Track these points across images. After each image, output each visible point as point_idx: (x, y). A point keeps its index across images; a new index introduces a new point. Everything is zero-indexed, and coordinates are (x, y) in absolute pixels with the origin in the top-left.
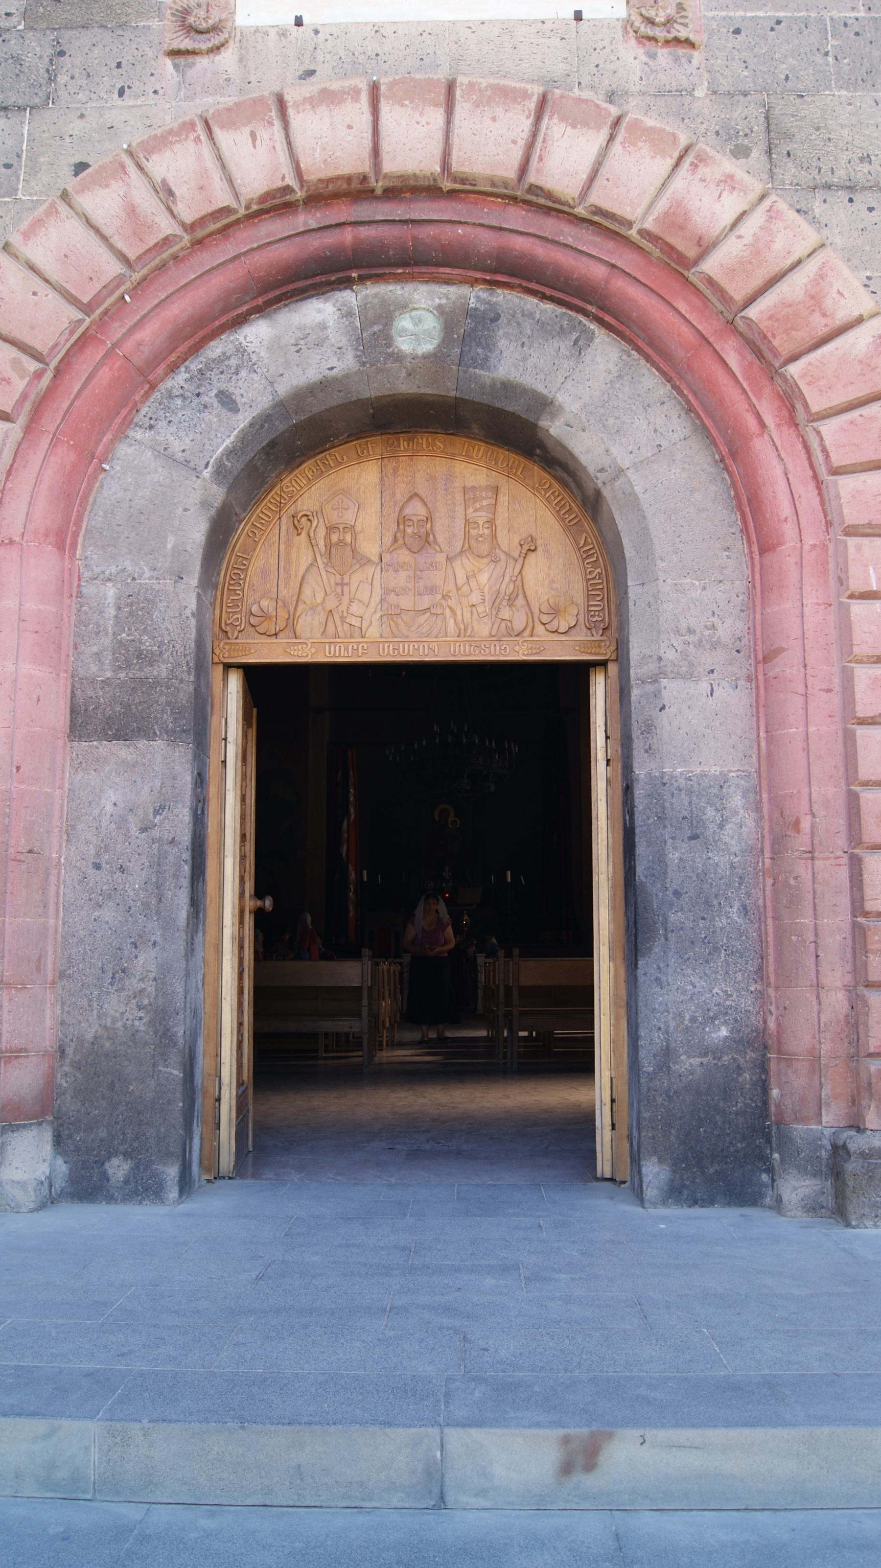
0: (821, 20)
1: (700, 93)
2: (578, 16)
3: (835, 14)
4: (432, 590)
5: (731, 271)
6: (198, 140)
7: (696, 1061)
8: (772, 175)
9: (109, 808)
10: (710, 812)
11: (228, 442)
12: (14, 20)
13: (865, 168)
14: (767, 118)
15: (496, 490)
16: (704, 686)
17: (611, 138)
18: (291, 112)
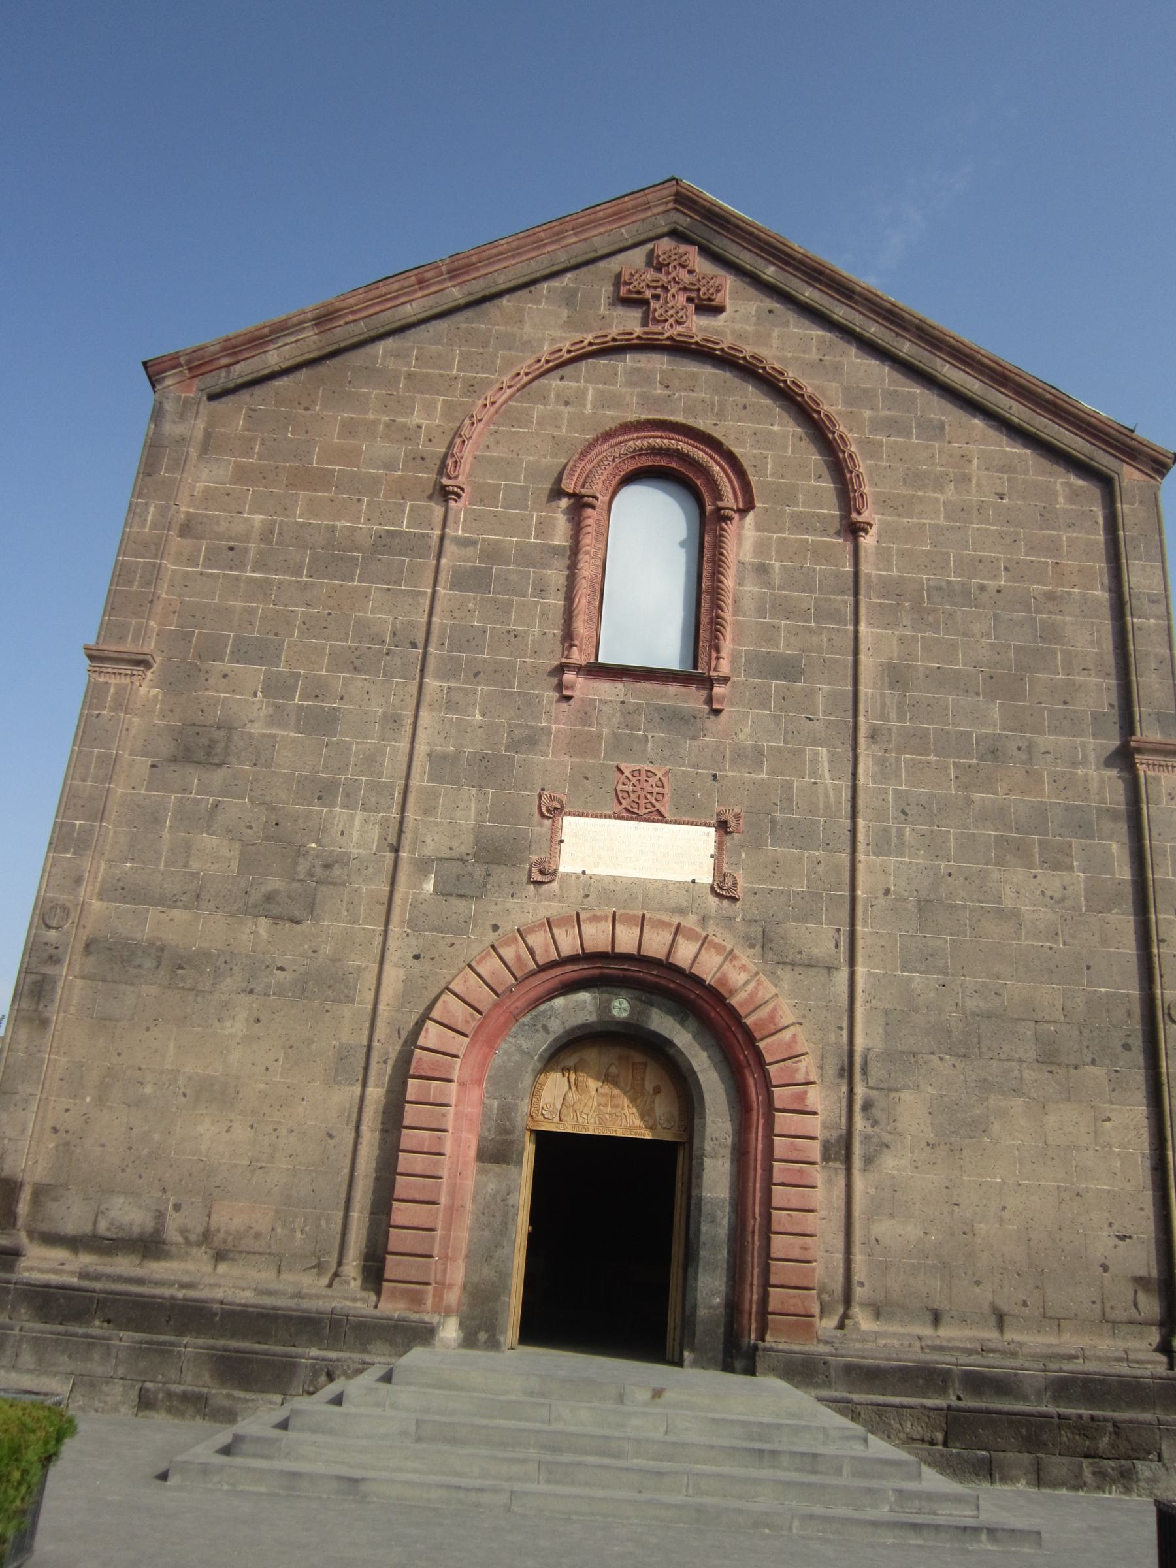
0: (788, 891)
1: (738, 919)
2: (693, 881)
3: (794, 889)
4: (617, 1106)
5: (741, 1004)
6: (545, 930)
7: (706, 1311)
8: (763, 956)
9: (490, 1191)
10: (719, 1212)
11: (545, 1046)
12: (471, 857)
13: (799, 956)
14: (764, 932)
15: (646, 1065)
16: (720, 1162)
17: (702, 944)
18: (582, 923)
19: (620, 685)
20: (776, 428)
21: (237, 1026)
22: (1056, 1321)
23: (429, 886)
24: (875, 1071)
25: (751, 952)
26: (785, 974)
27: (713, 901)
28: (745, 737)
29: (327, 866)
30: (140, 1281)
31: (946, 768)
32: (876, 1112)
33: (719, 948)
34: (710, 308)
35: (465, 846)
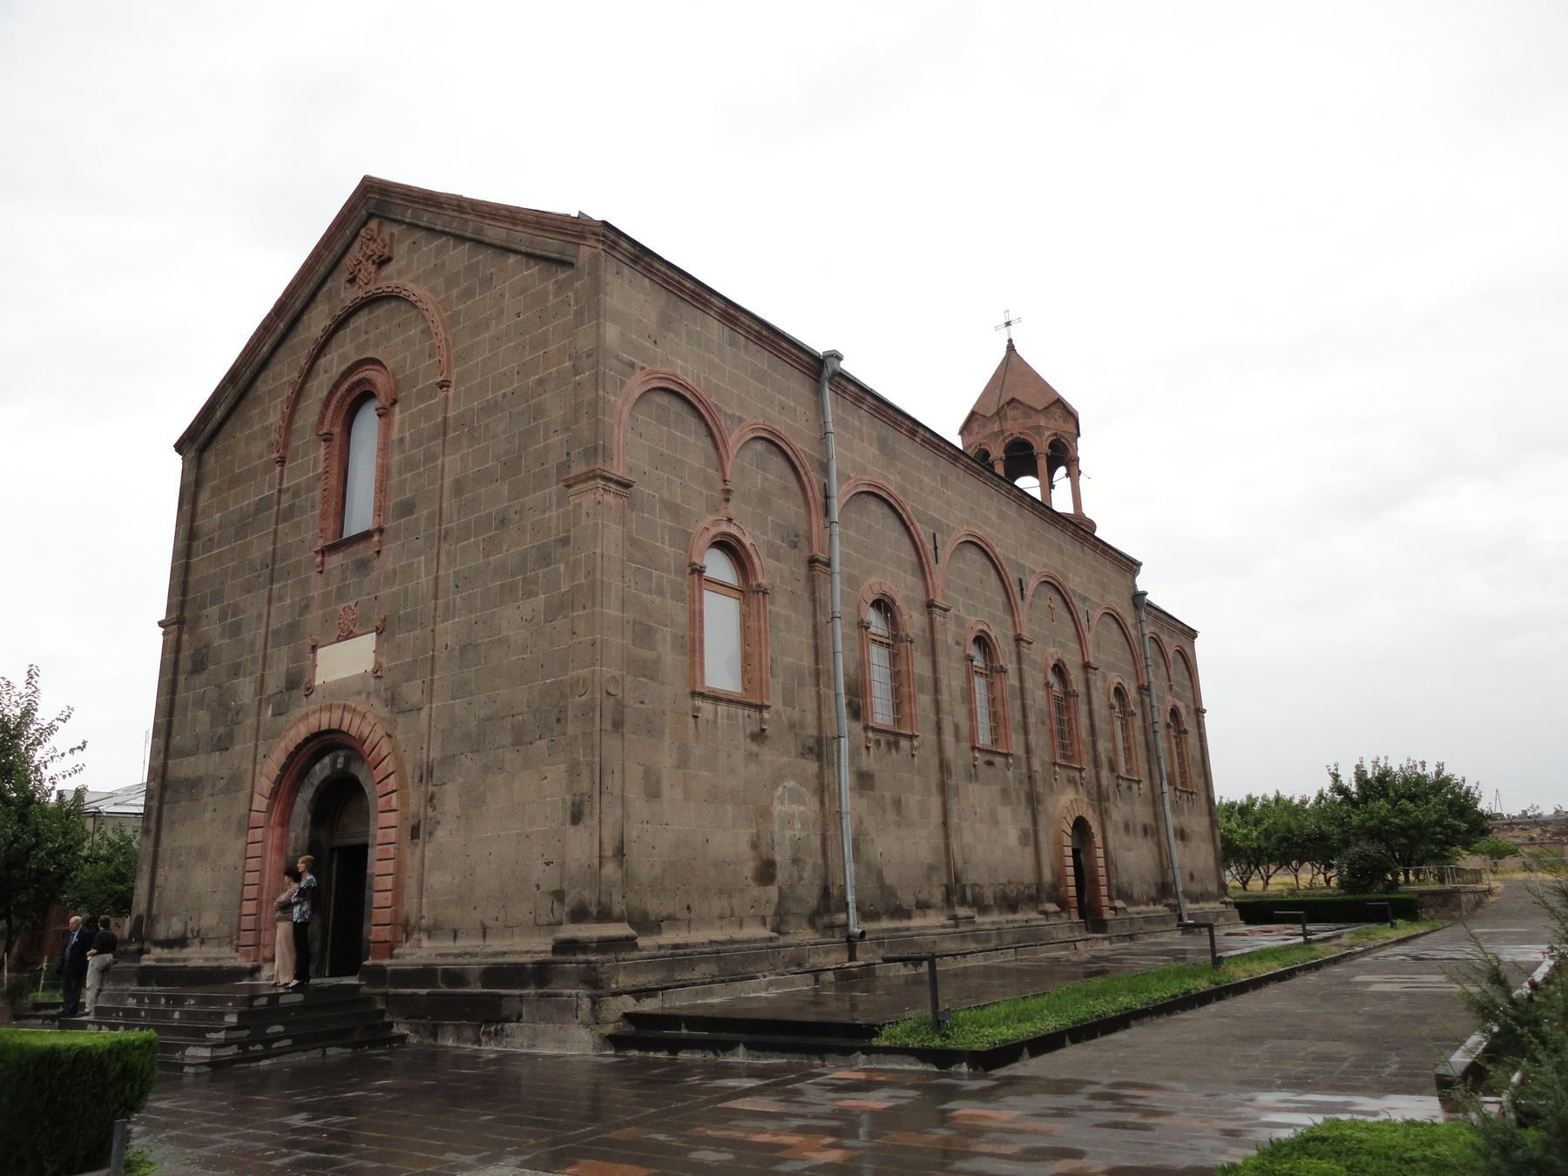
19: (341, 554)
20: (413, 332)
21: (208, 816)
22: (509, 929)
23: (270, 713)
24: (436, 774)
25: (386, 709)
26: (401, 720)
27: (373, 680)
28: (389, 566)
29: (237, 714)
30: (172, 960)
31: (479, 544)
32: (435, 801)
33: (359, 713)
34: (383, 262)
35: (282, 683)
